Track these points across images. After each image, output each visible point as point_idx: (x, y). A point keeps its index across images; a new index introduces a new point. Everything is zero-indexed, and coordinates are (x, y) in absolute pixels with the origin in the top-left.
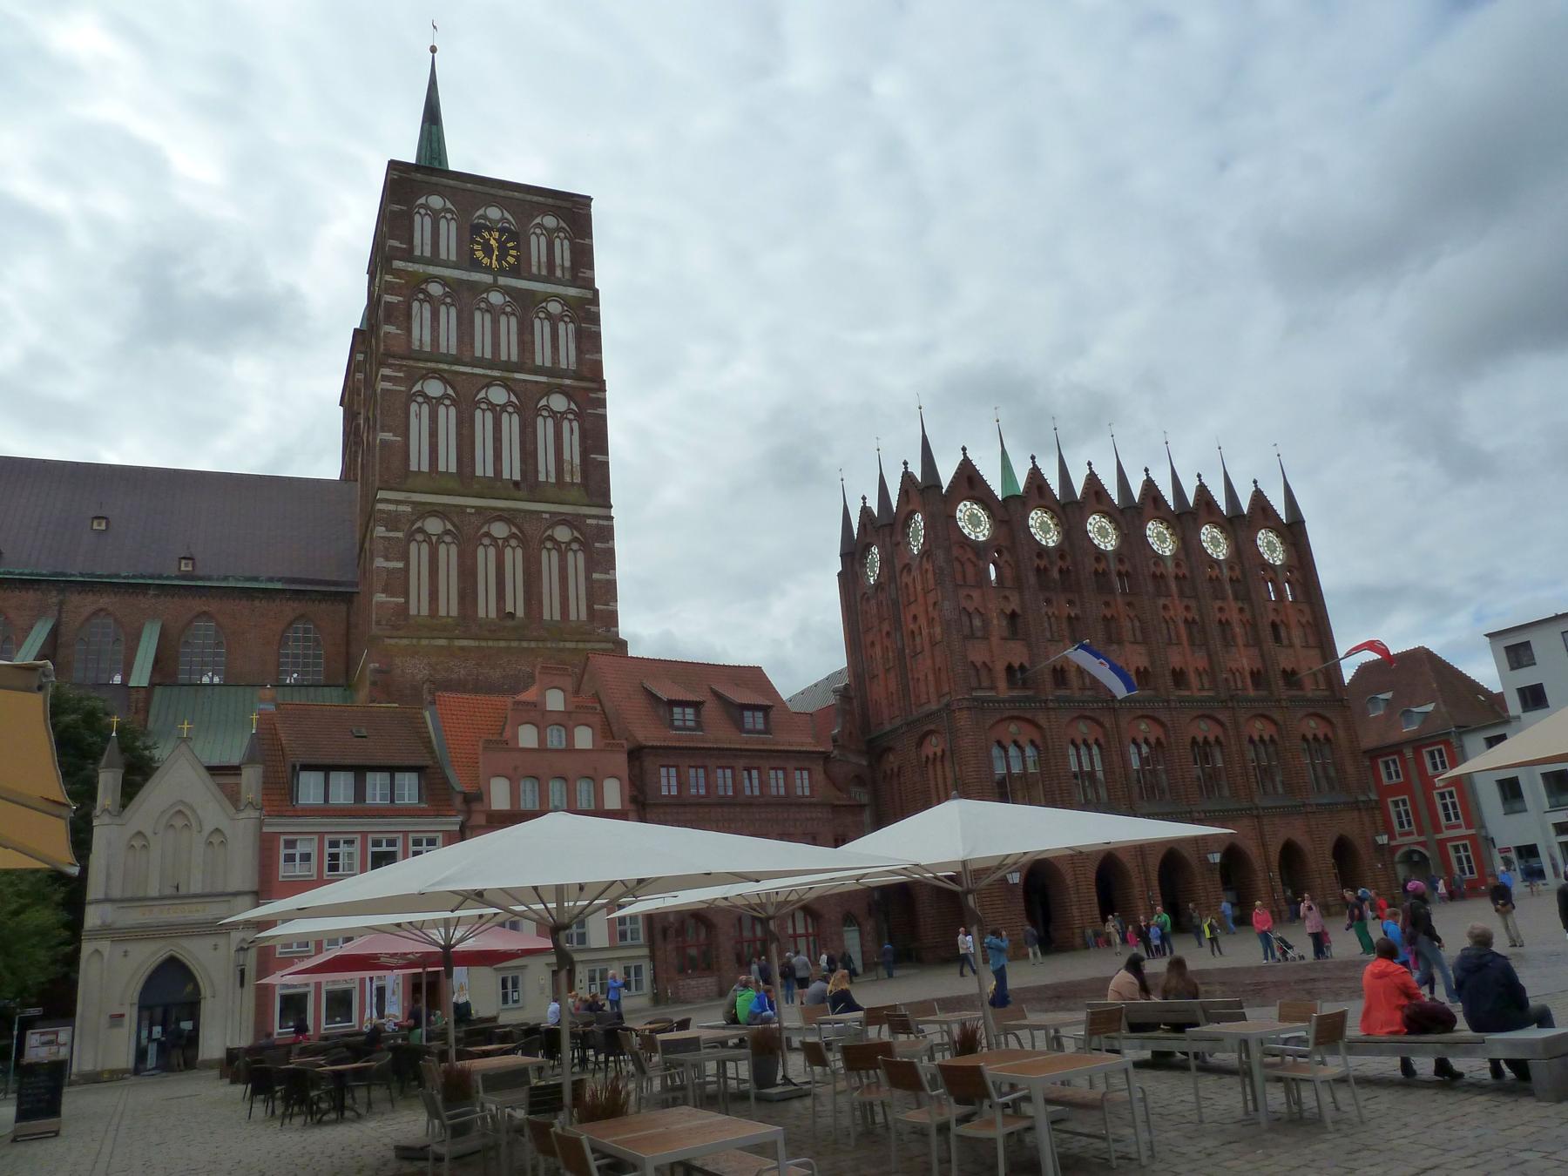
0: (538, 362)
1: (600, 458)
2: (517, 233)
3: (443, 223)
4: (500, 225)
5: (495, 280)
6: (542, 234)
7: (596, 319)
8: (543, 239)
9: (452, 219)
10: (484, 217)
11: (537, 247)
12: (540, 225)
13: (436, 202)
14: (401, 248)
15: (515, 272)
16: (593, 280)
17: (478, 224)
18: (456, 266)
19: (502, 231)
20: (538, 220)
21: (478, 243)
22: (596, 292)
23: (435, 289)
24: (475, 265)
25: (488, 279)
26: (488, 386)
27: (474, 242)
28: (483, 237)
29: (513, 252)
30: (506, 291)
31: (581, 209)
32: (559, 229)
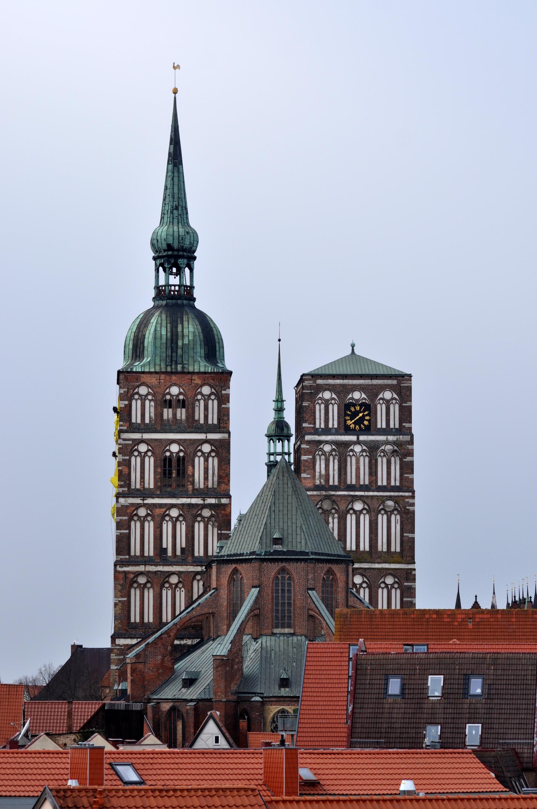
0: (380, 484)
1: (410, 535)
2: (370, 405)
3: (330, 407)
4: (361, 402)
5: (358, 438)
6: (383, 403)
7: (411, 453)
8: (384, 406)
9: (335, 403)
10: (352, 398)
11: (381, 409)
12: (383, 399)
13: (327, 395)
14: (309, 427)
15: (368, 430)
16: (410, 428)
17: (349, 403)
18: (337, 432)
19: (361, 405)
20: (381, 396)
21: (348, 415)
22: (412, 436)
23: (327, 448)
24: (347, 430)
25: (354, 438)
26: (352, 502)
27: (346, 415)
28: (351, 411)
29: (367, 418)
30: (365, 443)
31: (405, 383)
32: (393, 399)
